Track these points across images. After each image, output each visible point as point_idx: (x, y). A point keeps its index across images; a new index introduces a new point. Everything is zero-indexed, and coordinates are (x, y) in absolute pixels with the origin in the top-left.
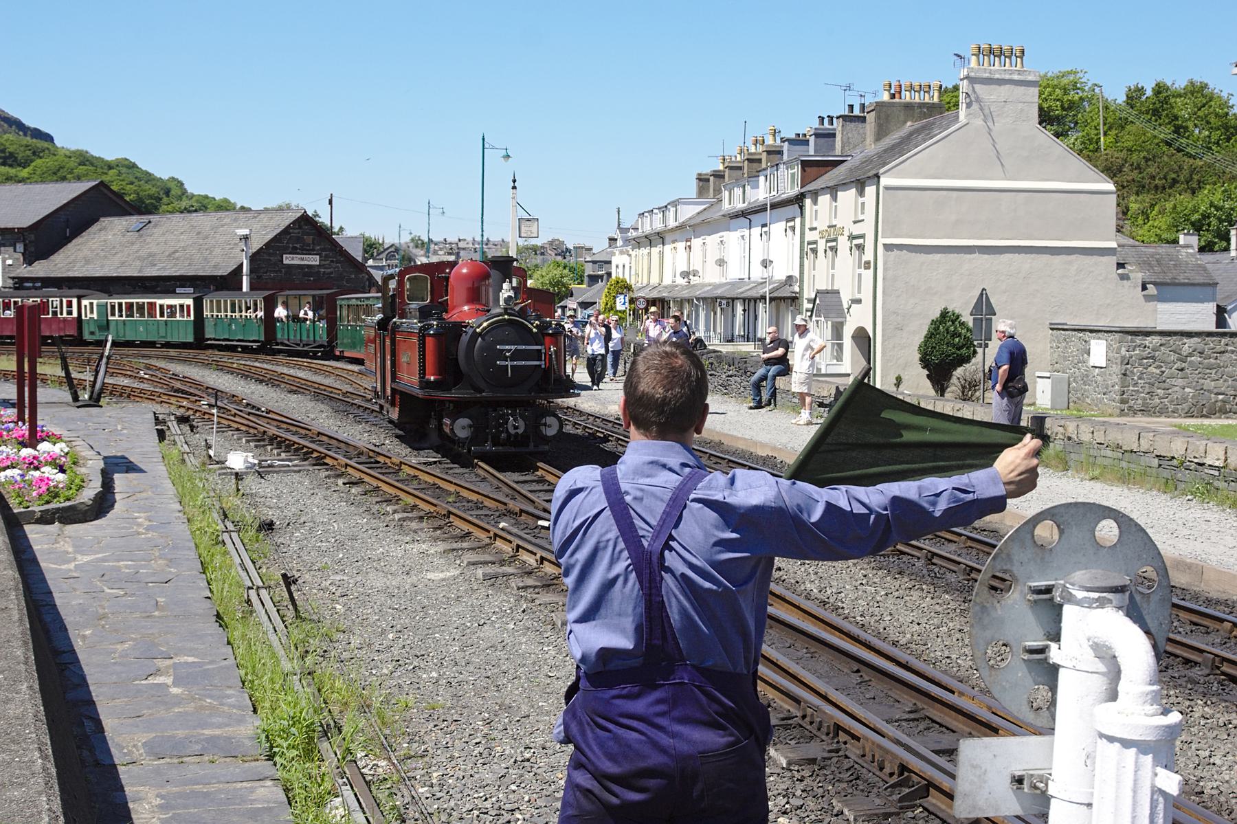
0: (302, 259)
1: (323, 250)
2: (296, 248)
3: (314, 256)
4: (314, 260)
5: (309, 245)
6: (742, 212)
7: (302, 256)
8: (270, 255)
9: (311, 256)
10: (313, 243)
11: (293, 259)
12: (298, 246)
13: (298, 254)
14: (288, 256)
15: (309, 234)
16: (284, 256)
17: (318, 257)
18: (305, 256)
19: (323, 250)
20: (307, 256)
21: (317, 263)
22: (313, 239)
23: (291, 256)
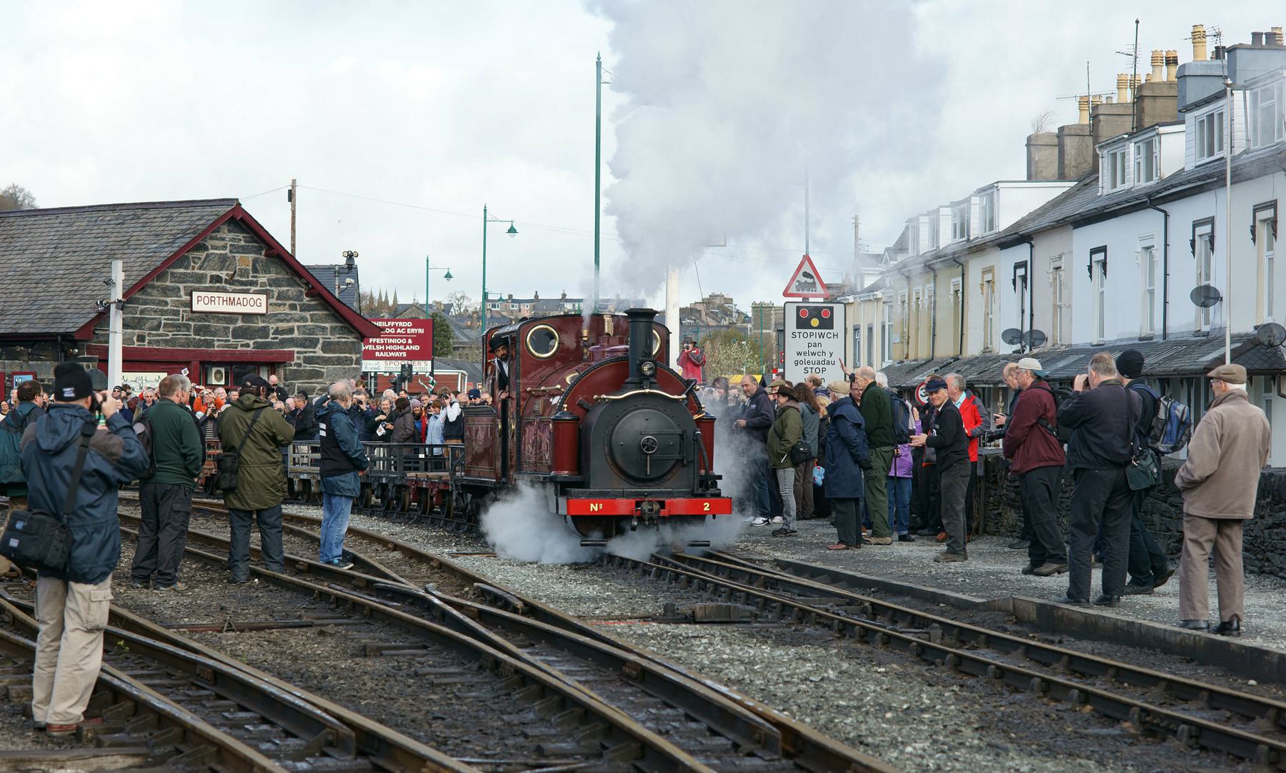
0: (232, 302)
1: (273, 283)
2: (218, 279)
3: (256, 297)
4: (254, 303)
5: (244, 273)
6: (1149, 195)
7: (232, 295)
8: (165, 291)
9: (248, 296)
10: (255, 270)
11: (212, 300)
12: (223, 274)
13: (225, 291)
14: (203, 294)
15: (244, 250)
16: (195, 294)
17: (263, 297)
18: (237, 296)
19: (273, 283)
20: (242, 296)
21: (262, 310)
22: (255, 261)
23: (210, 294)
